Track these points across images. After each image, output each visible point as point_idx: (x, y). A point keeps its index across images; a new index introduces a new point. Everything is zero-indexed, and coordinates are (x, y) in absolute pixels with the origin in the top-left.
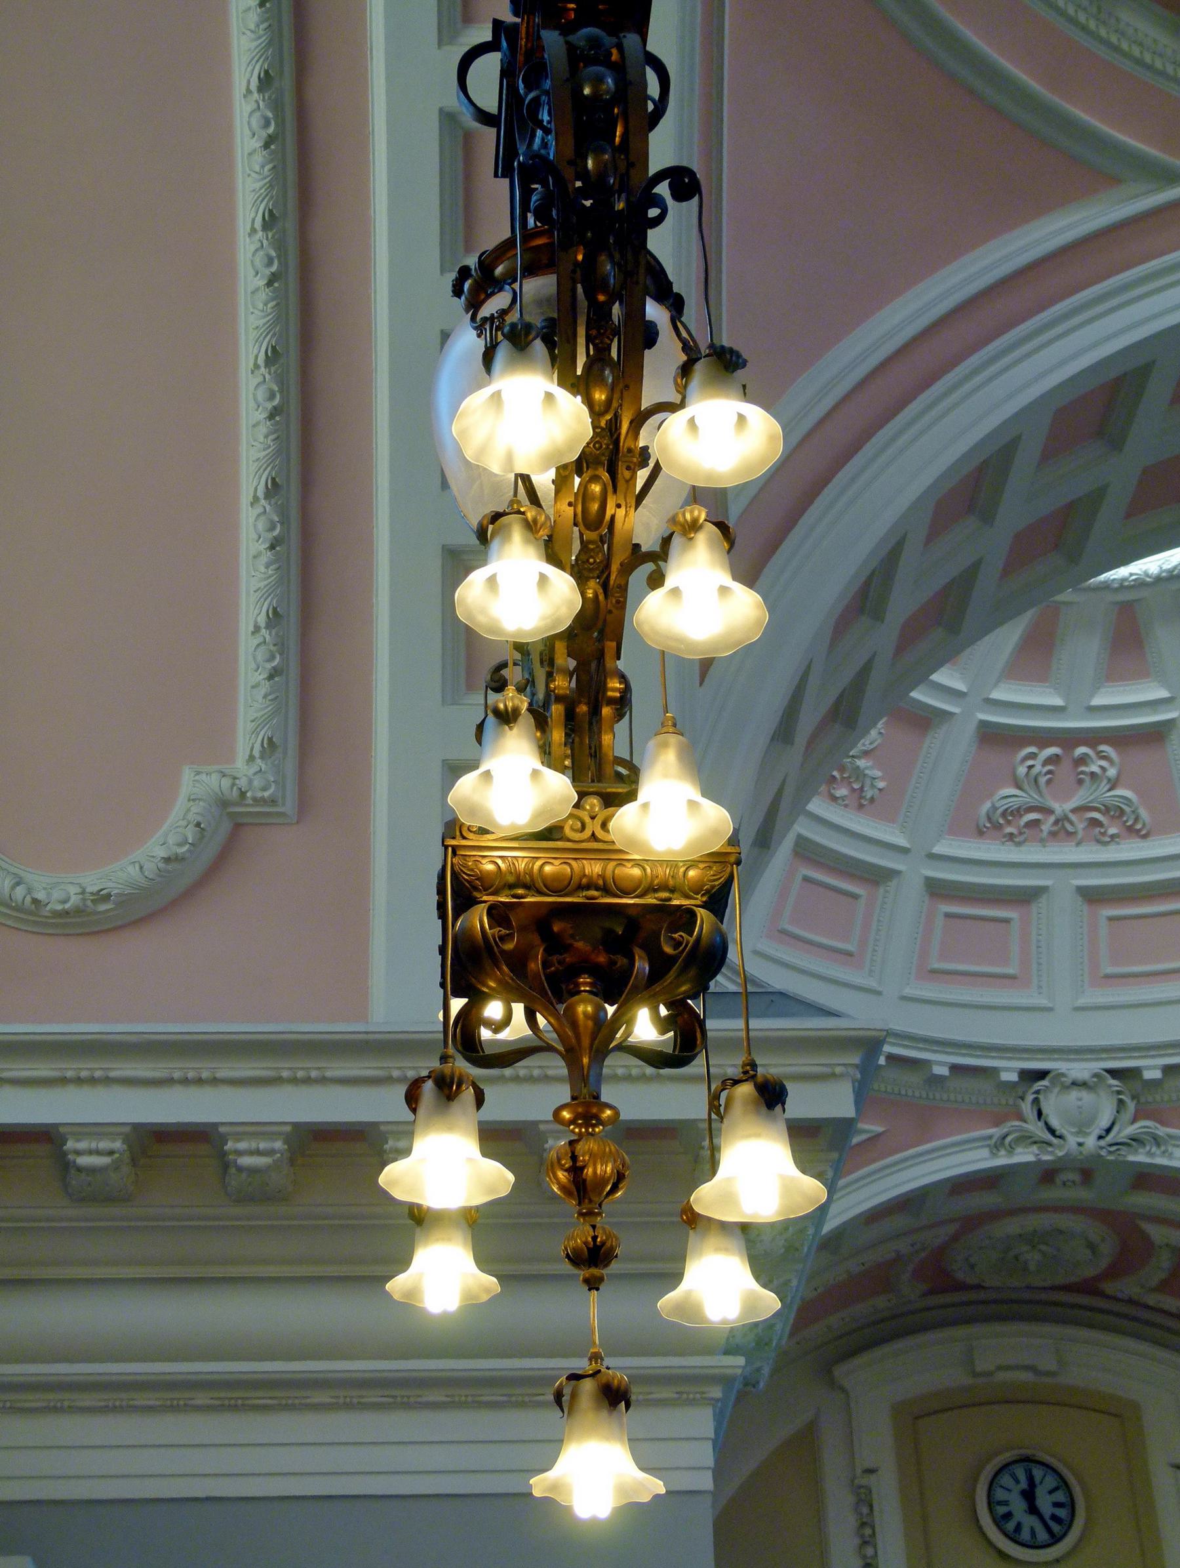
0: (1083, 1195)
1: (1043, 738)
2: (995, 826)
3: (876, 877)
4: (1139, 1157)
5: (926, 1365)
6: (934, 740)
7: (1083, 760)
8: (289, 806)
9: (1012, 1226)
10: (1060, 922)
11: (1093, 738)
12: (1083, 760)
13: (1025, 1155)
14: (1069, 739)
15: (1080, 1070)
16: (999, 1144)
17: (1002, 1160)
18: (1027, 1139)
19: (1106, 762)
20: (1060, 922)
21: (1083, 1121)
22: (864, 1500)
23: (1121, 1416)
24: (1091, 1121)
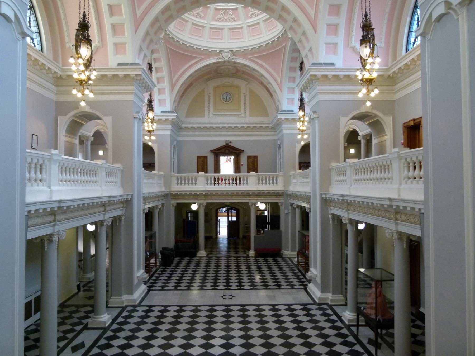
0: (229, 64)
1: (223, 9)
2: (219, 20)
3: (203, 27)
4: (233, 61)
5: (218, 82)
6: (209, 10)
7: (228, 12)
8: (101, 47)
9: (223, 67)
10: (226, 32)
11: (229, 9)
12: (228, 12)
13: (220, 60)
14: (226, 9)
15: (226, 50)
16: (217, 59)
17: (218, 61)
18: (221, 59)
19: (230, 12)
20: (226, 32)
21: (226, 56)
22: (209, 97)
23: (238, 88)
24: (228, 56)
